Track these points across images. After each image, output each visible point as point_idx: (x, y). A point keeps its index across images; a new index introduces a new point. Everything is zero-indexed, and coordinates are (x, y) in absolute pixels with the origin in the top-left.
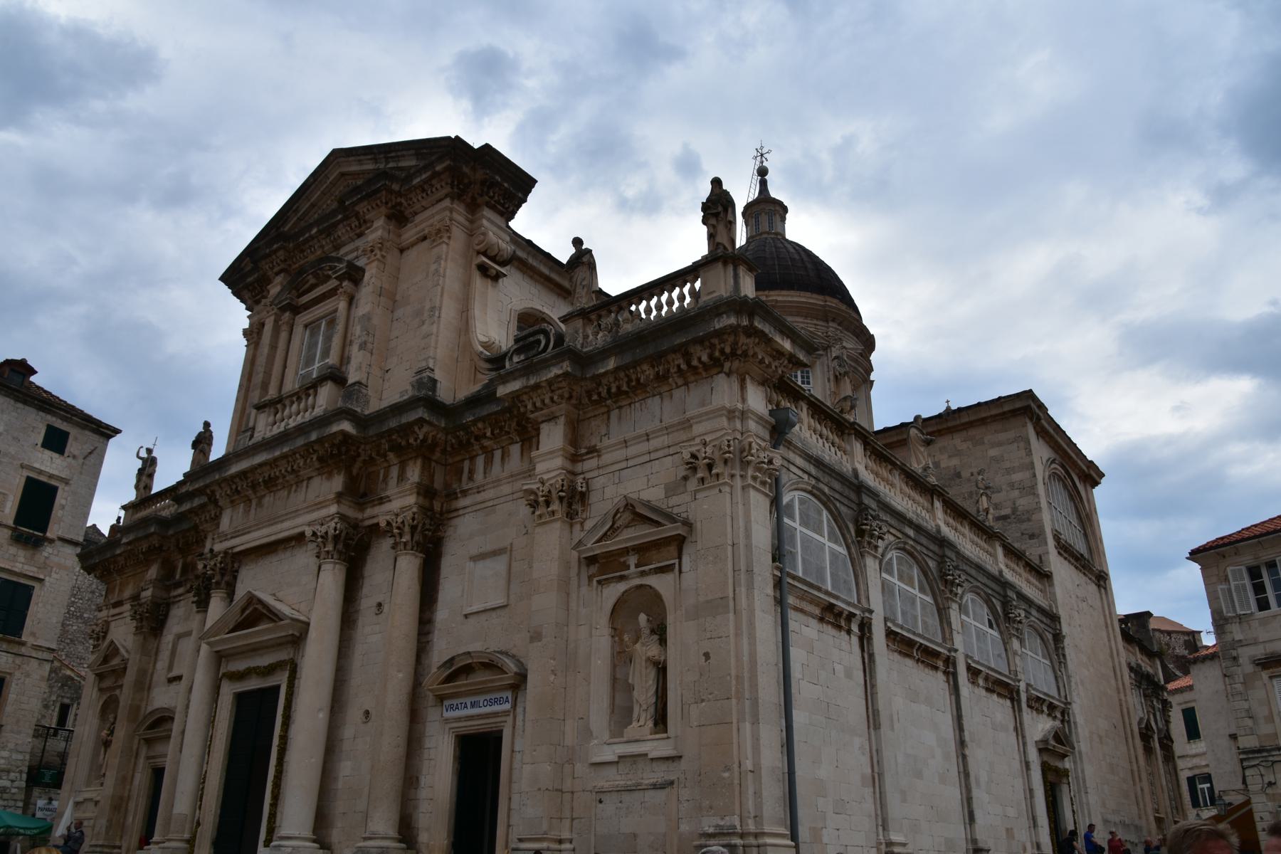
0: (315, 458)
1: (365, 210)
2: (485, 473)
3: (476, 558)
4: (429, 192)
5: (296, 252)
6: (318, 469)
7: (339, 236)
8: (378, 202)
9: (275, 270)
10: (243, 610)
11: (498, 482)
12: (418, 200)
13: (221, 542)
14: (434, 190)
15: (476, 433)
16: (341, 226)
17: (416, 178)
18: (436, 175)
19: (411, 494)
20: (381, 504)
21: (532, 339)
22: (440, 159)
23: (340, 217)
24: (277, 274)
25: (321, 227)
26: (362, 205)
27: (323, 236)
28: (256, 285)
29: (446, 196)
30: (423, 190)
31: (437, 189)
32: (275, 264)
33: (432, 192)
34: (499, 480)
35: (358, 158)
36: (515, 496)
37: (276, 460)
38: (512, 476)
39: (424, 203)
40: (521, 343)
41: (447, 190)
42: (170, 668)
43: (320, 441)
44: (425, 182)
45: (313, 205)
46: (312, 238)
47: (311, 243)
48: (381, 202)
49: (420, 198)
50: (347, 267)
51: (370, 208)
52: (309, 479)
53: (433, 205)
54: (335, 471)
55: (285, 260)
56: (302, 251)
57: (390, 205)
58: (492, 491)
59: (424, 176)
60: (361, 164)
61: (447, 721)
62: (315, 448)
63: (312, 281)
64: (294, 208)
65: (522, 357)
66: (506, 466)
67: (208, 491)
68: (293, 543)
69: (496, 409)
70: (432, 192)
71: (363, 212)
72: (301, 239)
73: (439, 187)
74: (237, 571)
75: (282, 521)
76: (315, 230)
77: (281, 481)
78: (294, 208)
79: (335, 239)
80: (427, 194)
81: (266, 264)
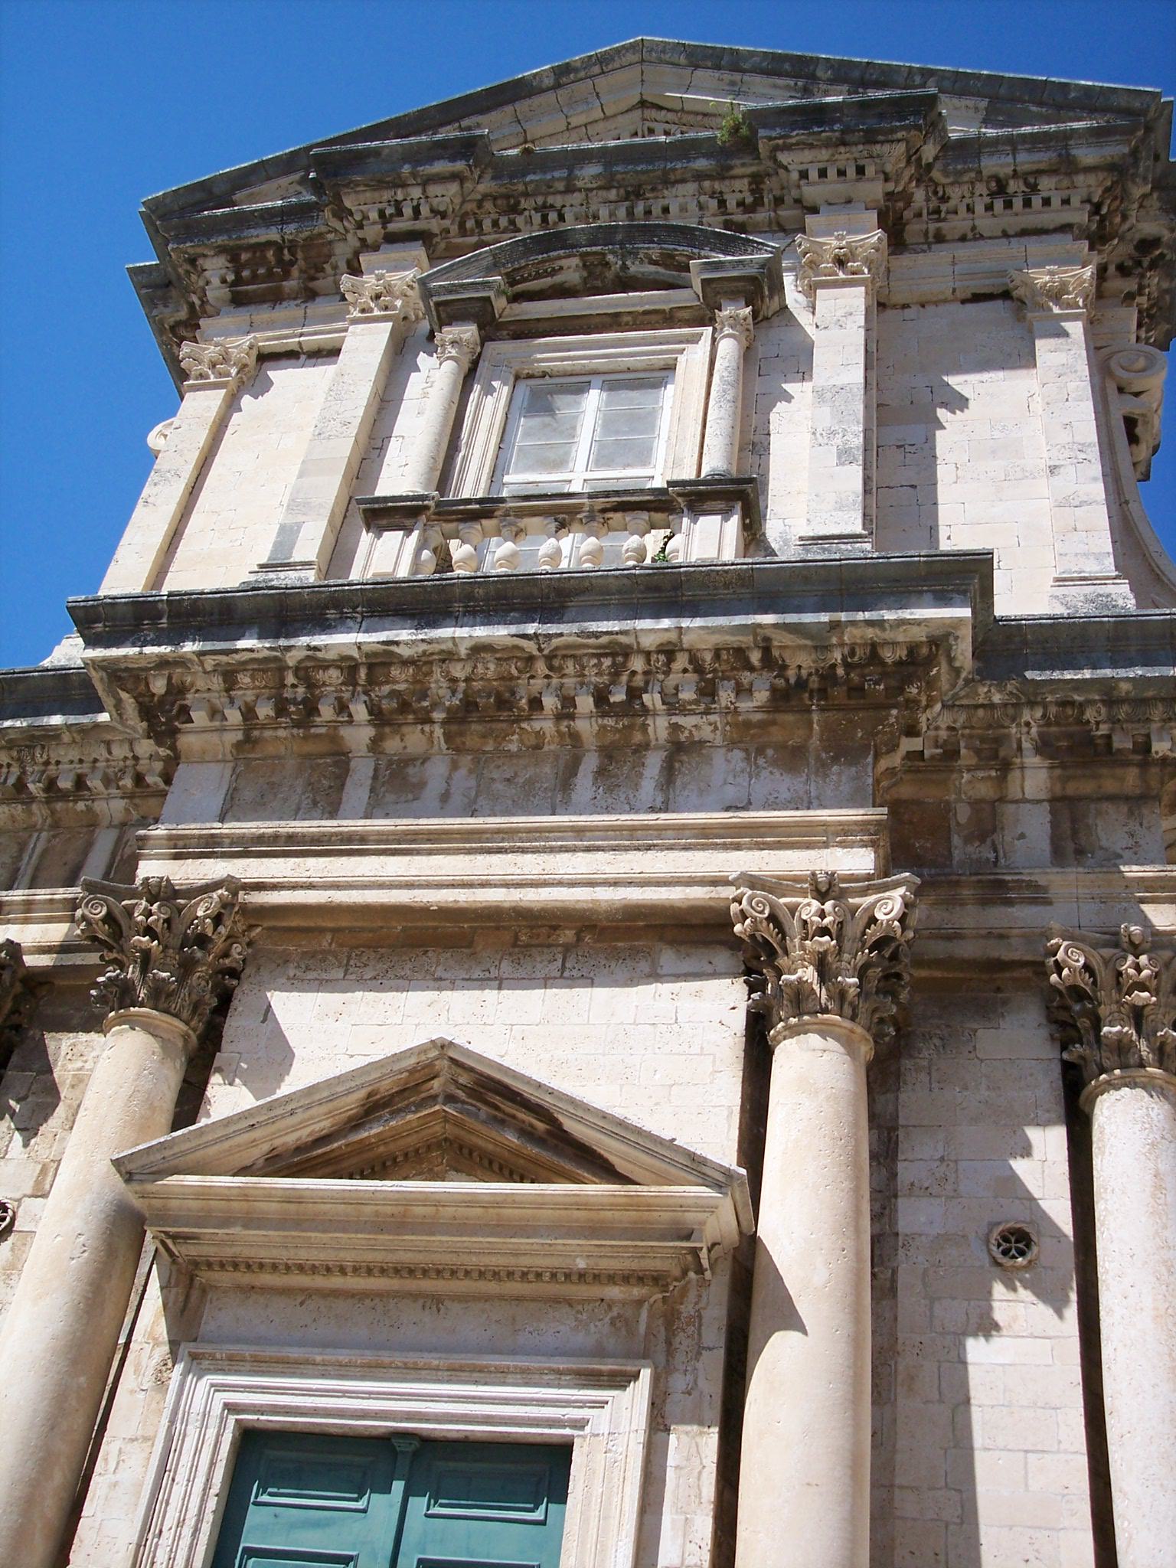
4: (1018, 203)
5: (488, 205)
9: (393, 227)
12: (970, 209)
14: (1036, 201)
16: (691, 187)
17: (992, 154)
18: (1067, 167)
20: (984, 902)
24: (392, 239)
26: (807, 155)
27: (613, 194)
28: (270, 254)
29: (1065, 228)
31: (1047, 202)
33: (1027, 203)
35: (737, 76)
39: (985, 223)
41: (1079, 216)
49: (979, 208)
50: (763, 265)
57: (890, 187)
63: (571, 271)
70: (1027, 203)
74: (234, 973)
80: (1008, 205)
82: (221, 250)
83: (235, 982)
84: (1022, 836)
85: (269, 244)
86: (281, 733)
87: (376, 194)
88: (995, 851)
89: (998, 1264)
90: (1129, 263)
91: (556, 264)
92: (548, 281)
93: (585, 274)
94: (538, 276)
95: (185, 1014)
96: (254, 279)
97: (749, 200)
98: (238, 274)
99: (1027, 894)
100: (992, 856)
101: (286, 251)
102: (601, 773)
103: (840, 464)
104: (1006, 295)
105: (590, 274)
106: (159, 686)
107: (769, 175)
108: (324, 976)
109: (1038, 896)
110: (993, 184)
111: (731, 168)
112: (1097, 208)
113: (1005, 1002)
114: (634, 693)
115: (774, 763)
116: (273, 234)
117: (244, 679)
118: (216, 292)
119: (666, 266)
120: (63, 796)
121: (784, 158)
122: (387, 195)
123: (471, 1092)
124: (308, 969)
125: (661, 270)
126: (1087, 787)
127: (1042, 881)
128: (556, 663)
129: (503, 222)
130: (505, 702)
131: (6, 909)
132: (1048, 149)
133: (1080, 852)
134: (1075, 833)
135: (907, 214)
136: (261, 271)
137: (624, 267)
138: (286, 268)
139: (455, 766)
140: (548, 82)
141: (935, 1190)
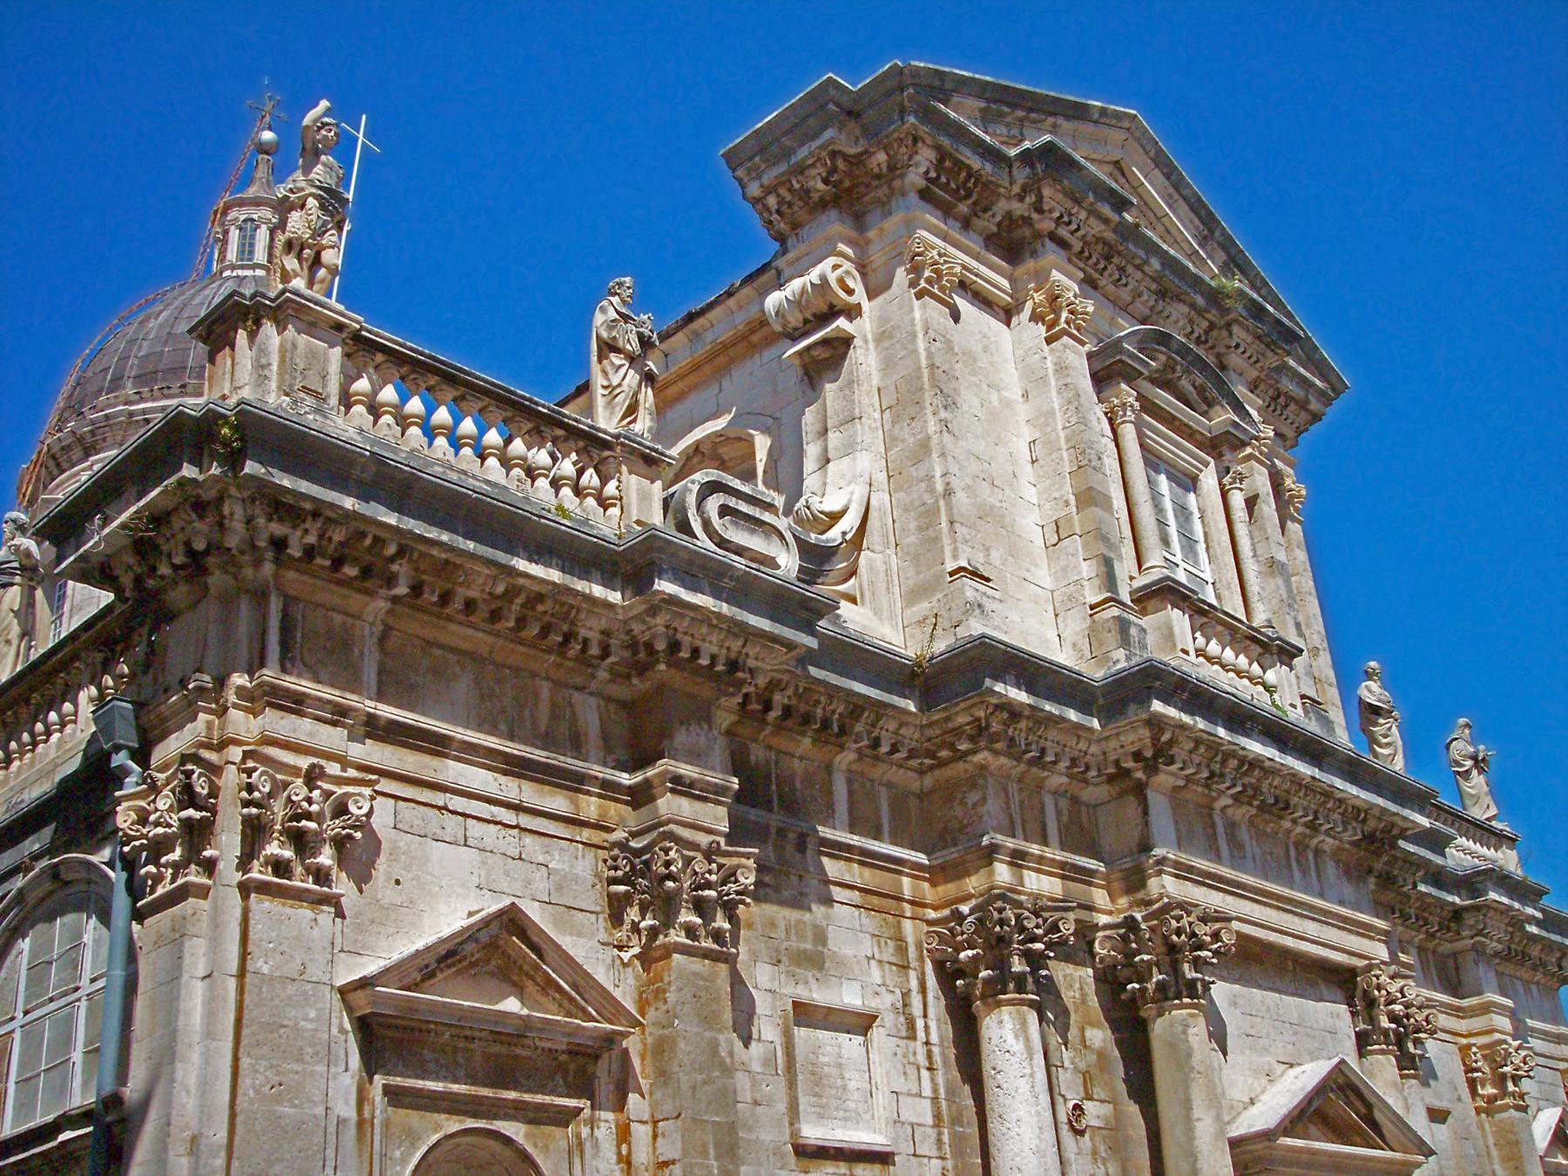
16: (1186, 309)
27: (1154, 286)
47: (1130, 269)
82: (938, 148)
85: (969, 167)
96: (946, 186)
101: (973, 180)
111: (1209, 312)
116: (975, 163)
117: (1202, 749)
118: (915, 178)
119: (1198, 394)
121: (1236, 329)
122: (1069, 204)
123: (1341, 1088)
130: (1287, 807)
131: (1028, 858)
137: (1180, 378)
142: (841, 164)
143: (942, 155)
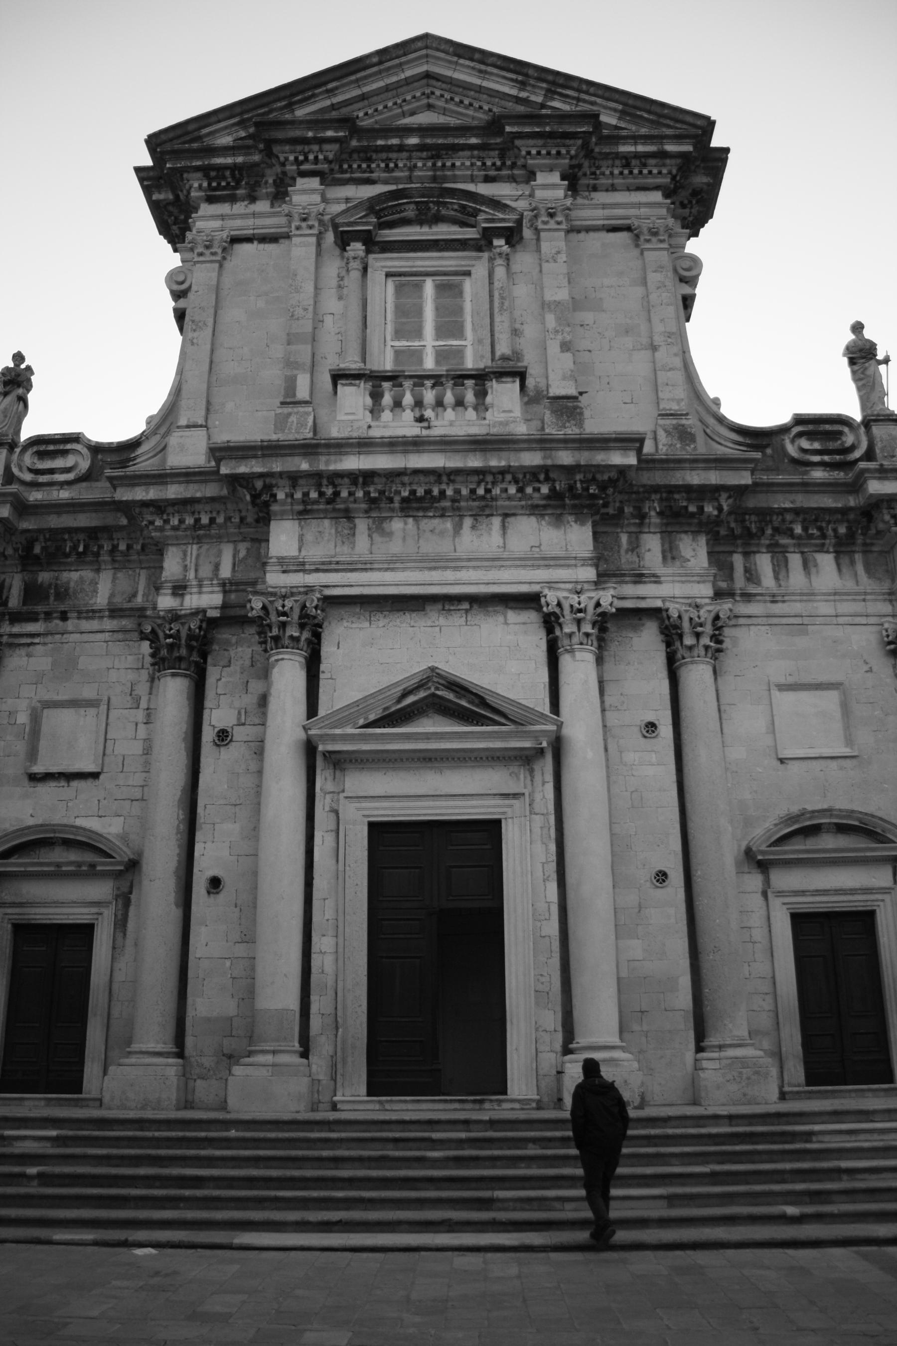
0: (545, 490)
1: (534, 152)
2: (777, 578)
3: (782, 688)
4: (636, 171)
6: (537, 506)
7: (453, 165)
8: (563, 151)
9: (303, 167)
10: (405, 694)
11: (809, 595)
12: (612, 173)
13: (284, 572)
15: (776, 524)
16: (467, 153)
17: (624, 144)
19: (704, 582)
20: (635, 583)
21: (828, 427)
22: (678, 138)
23: (474, 141)
24: (304, 174)
25: (429, 141)
26: (531, 142)
27: (424, 154)
28: (228, 173)
29: (657, 188)
30: (627, 165)
32: (311, 157)
33: (641, 172)
34: (813, 594)
36: (841, 620)
37: (451, 475)
38: (835, 594)
39: (618, 181)
40: (810, 427)
42: (33, 754)
43: (569, 470)
44: (637, 155)
45: (363, 97)
46: (401, 148)
47: (394, 155)
48: (568, 152)
51: (544, 152)
52: (506, 516)
53: (628, 190)
54: (571, 518)
55: (330, 162)
56: (369, 160)
58: (798, 605)
59: (641, 148)
60: (484, 79)
61: (780, 894)
62: (552, 475)
63: (410, 212)
64: (330, 86)
65: (817, 446)
66: (813, 577)
67: (259, 484)
68: (466, 606)
69: (834, 505)
70: (641, 172)
71: (529, 153)
72: (380, 142)
73: (655, 171)
75: (456, 568)
76: (413, 141)
77: (447, 504)
78: (330, 86)
79: (444, 165)
80: (631, 173)
81: (292, 152)
83: (320, 630)
84: (649, 550)
85: (225, 167)
86: (322, 507)
87: (293, 148)
88: (638, 557)
89: (645, 737)
90: (686, 202)
91: (402, 208)
92: (397, 216)
93: (417, 212)
94: (394, 214)
95: (305, 648)
97: (499, 163)
98: (209, 184)
99: (653, 579)
100: (637, 560)
101: (237, 172)
102: (473, 527)
103: (562, 351)
104: (628, 229)
105: (420, 213)
106: (259, 484)
107: (509, 150)
108: (360, 626)
109: (656, 579)
110: (624, 161)
112: (674, 178)
113: (643, 625)
114: (488, 491)
115: (549, 524)
119: (462, 213)
120: (203, 527)
122: (299, 148)
124: (352, 622)
125: (458, 214)
126: (677, 528)
127: (658, 572)
128: (452, 477)
129: (364, 166)
132: (652, 144)
133: (673, 558)
134: (671, 549)
135: (580, 174)
136: (223, 184)
137: (438, 210)
138: (238, 182)
139: (406, 524)
140: (375, 60)
141: (619, 707)
142: (171, 208)
143: (205, 170)
